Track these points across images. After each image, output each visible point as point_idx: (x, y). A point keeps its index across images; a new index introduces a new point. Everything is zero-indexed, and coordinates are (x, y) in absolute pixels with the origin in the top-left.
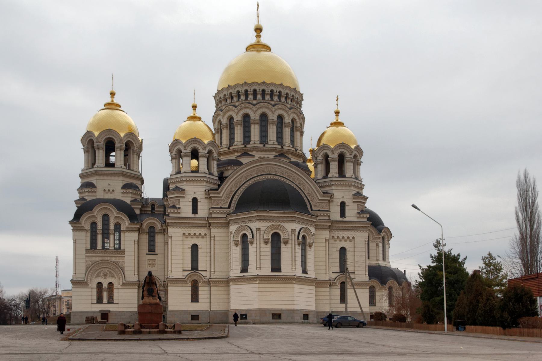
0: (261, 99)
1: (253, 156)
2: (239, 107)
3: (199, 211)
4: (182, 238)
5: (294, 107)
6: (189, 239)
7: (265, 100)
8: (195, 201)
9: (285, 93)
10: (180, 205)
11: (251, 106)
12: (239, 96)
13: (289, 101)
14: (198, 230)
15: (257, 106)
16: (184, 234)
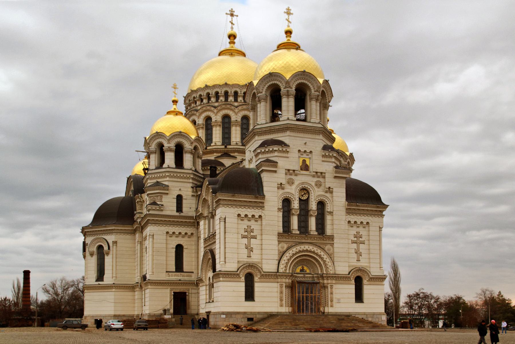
1: (235, 157)
3: (184, 209)
4: (165, 236)
6: (174, 238)
8: (179, 199)
10: (162, 202)
14: (184, 228)
16: (167, 233)
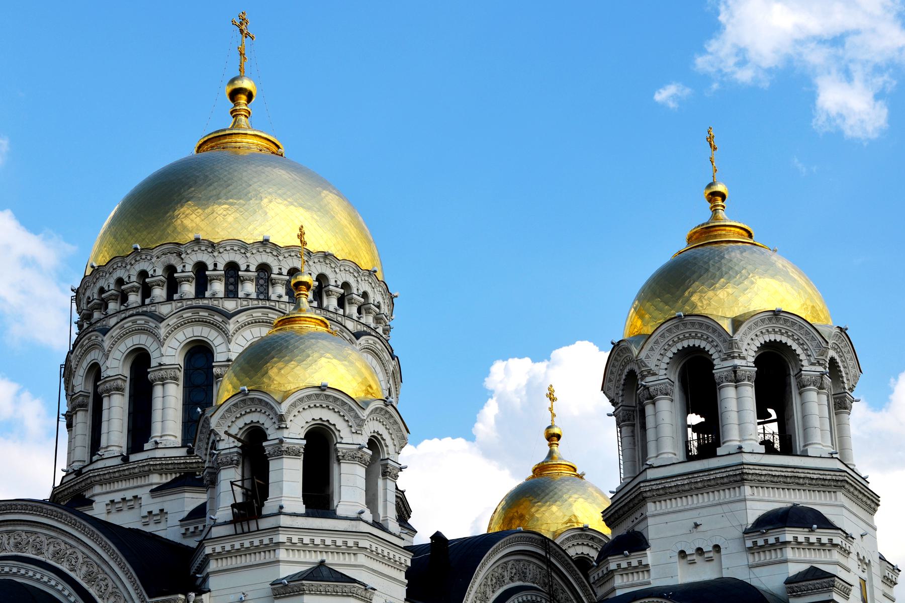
0: (254, 296)
2: (172, 321)
5: (369, 330)
7: (269, 299)
9: (340, 283)
11: (218, 318)
12: (173, 286)
13: (352, 310)
15: (242, 318)
